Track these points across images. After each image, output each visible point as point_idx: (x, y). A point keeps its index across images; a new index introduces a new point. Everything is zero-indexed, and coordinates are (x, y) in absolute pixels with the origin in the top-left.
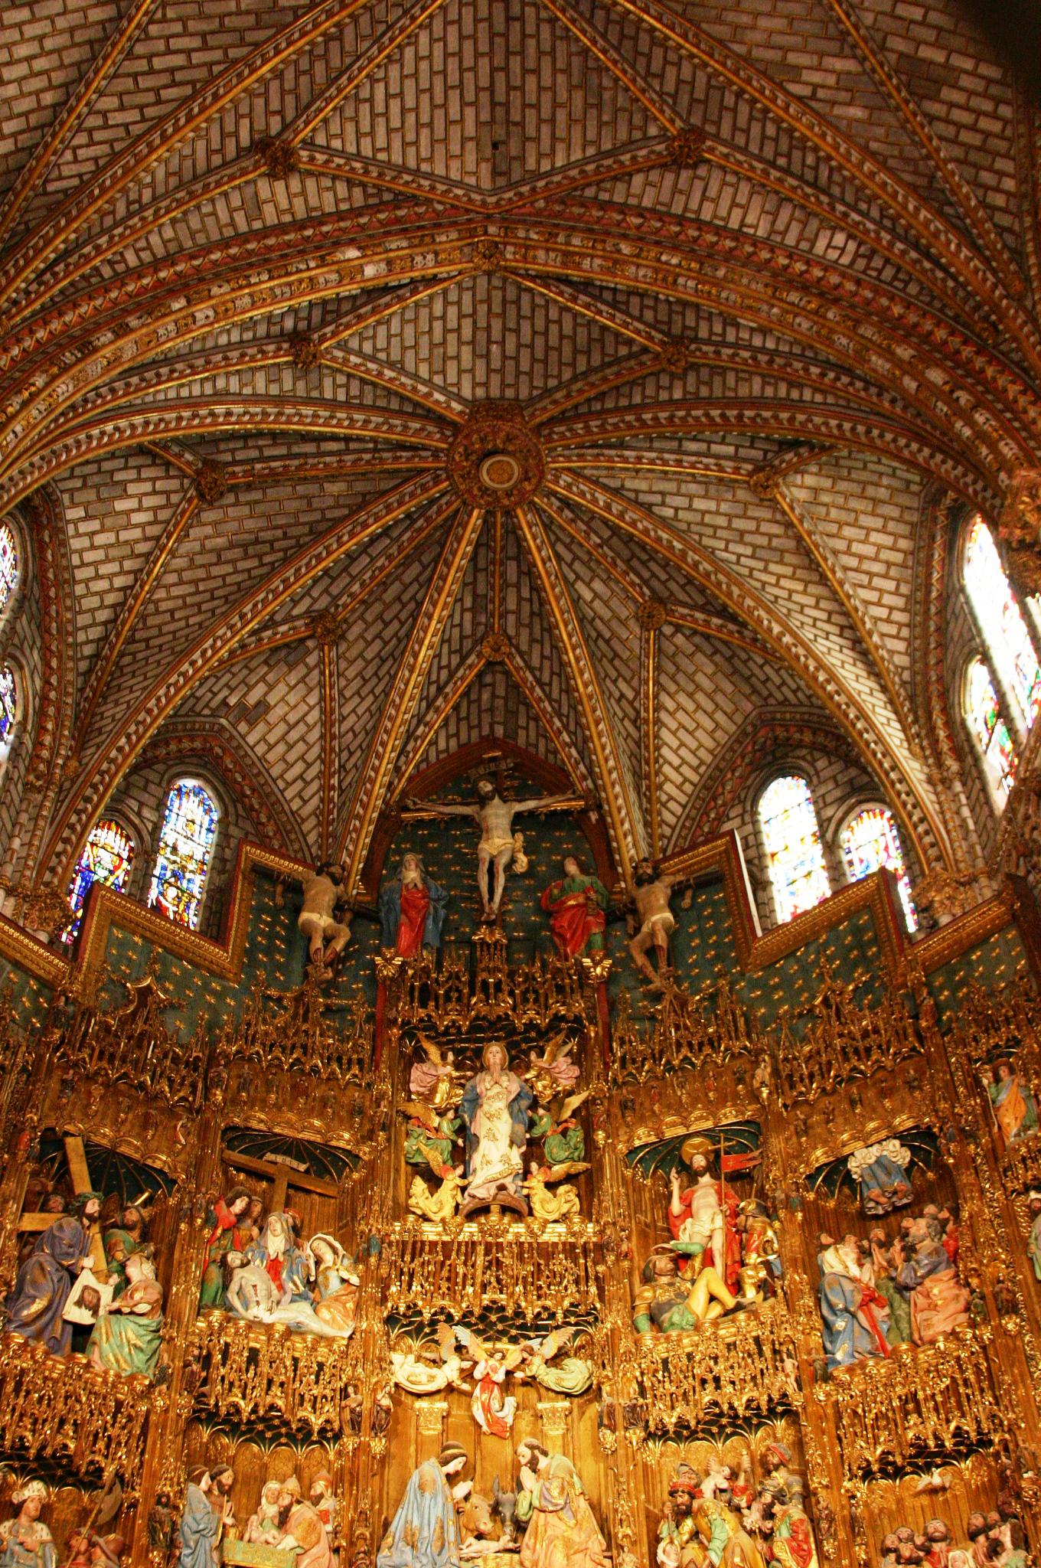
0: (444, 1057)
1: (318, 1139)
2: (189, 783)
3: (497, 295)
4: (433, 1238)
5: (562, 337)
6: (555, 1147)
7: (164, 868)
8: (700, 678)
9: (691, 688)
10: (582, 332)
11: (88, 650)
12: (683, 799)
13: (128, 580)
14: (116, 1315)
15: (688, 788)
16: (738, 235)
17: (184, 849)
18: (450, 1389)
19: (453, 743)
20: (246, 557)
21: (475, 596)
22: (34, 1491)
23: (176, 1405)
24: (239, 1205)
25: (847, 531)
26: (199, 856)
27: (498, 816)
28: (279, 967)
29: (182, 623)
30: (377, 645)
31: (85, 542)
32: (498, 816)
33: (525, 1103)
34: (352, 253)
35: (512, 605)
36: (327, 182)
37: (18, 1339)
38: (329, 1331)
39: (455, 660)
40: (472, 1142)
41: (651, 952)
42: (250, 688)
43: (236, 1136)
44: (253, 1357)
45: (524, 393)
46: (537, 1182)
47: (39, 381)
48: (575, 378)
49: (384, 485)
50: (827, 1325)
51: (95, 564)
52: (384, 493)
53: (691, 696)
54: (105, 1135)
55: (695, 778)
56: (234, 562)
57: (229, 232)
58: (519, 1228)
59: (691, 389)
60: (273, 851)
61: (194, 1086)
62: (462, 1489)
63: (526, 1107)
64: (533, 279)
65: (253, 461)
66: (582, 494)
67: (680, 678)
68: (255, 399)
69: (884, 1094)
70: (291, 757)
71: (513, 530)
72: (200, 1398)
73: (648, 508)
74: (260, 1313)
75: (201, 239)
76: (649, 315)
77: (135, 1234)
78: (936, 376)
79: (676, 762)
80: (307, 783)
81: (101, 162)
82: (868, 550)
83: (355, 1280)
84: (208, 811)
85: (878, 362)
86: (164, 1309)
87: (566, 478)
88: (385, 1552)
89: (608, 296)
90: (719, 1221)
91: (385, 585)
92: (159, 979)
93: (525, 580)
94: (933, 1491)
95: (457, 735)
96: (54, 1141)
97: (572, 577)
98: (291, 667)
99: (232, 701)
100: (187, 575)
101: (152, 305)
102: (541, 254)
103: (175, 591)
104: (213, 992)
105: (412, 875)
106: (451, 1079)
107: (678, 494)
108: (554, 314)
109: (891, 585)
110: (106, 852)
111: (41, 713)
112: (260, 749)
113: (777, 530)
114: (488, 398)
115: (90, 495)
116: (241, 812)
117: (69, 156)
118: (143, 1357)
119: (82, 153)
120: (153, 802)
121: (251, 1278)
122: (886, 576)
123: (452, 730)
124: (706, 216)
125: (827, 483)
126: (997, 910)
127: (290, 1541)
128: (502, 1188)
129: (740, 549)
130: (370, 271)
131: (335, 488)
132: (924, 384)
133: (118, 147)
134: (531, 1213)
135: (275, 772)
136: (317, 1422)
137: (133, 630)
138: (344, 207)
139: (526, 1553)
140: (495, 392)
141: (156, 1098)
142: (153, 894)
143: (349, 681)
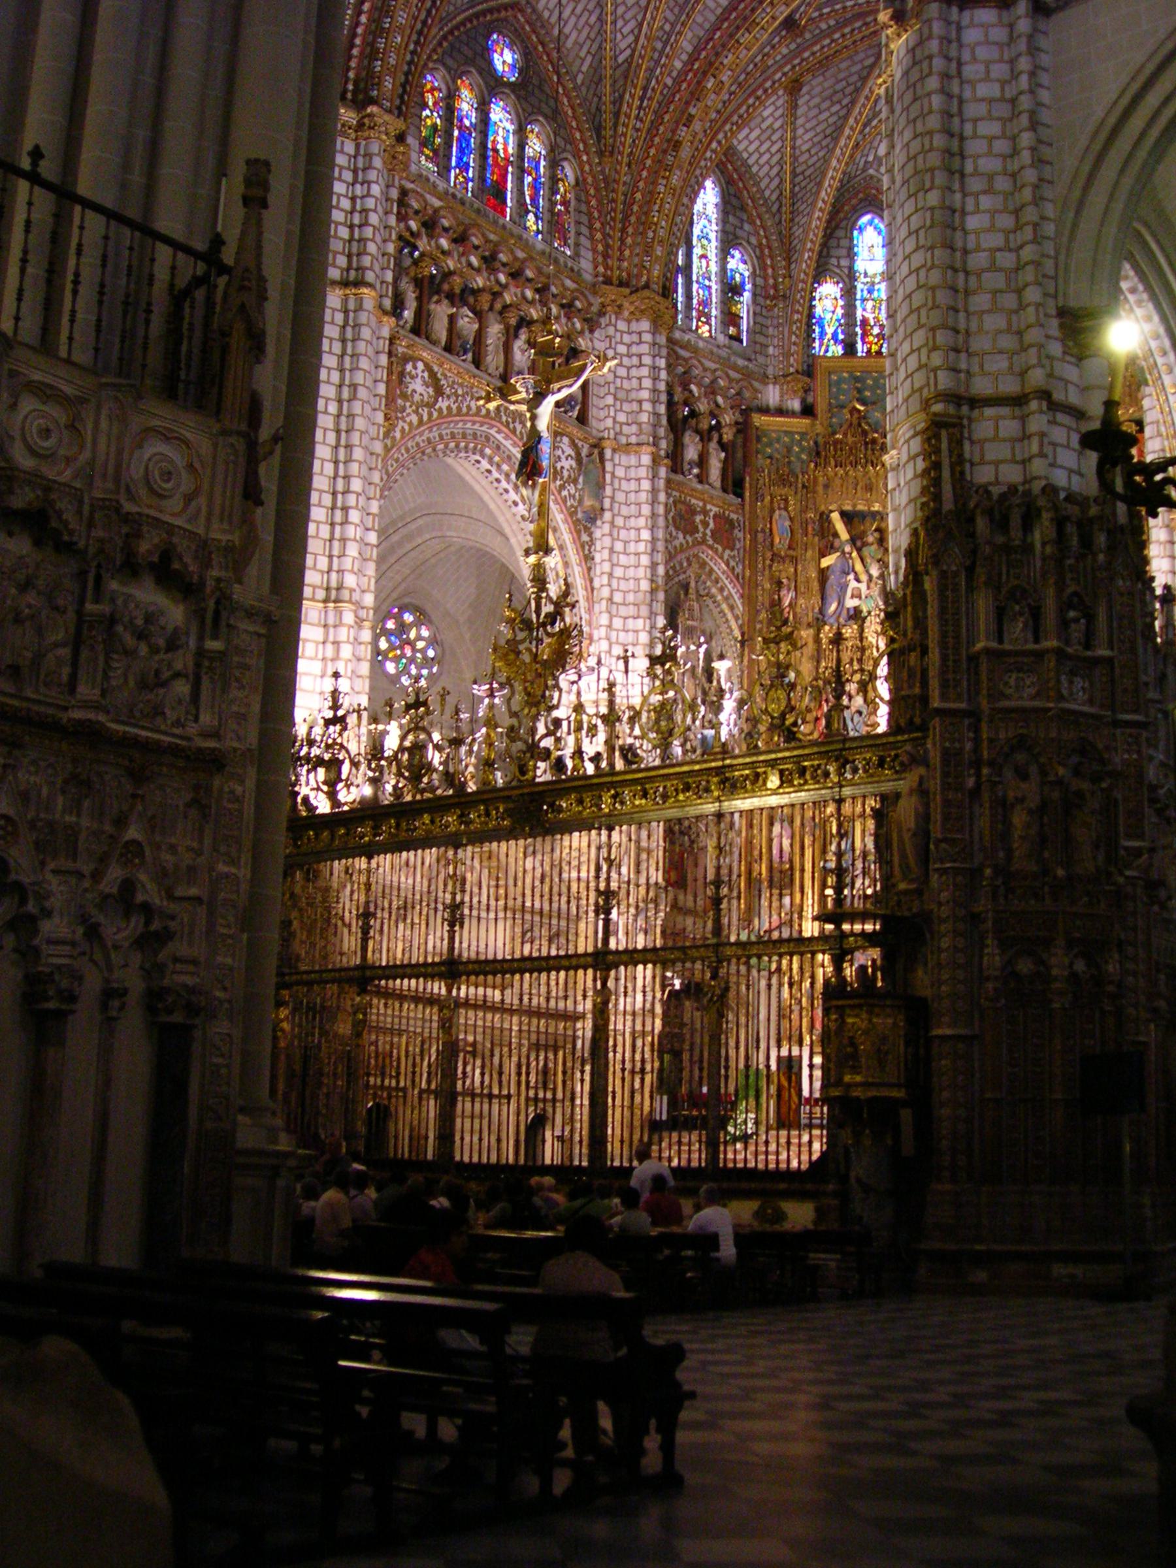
2: (865, 219)
11: (774, 197)
13: (779, 145)
20: (833, 104)
31: (746, 143)
51: (757, 149)
56: (828, 109)
68: (787, 59)
75: (707, 26)
100: (808, 126)
101: (697, 94)
103: (806, 137)
111: (761, 258)
117: (619, 36)
120: (844, 252)
133: (639, 18)
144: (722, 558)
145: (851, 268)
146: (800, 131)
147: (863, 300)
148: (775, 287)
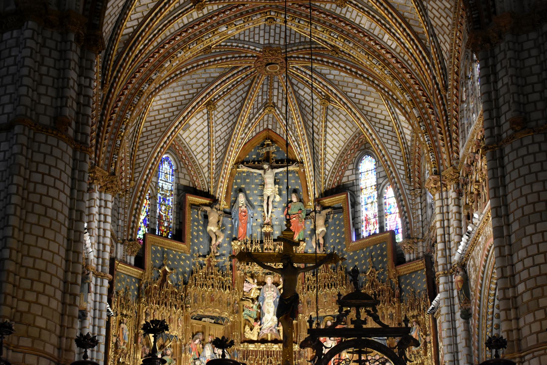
4: (252, 349)
7: (160, 198)
8: (341, 116)
9: (338, 119)
12: (333, 160)
15: (335, 156)
17: (165, 187)
20: (183, 90)
21: (263, 92)
28: (201, 243)
29: (162, 116)
32: (269, 177)
53: (337, 122)
56: (179, 92)
67: (334, 116)
70: (199, 143)
79: (331, 146)
81: (140, 20)
97: (297, 89)
103: (159, 103)
114: (269, 43)
116: (182, 166)
119: (133, 17)
133: (145, 13)
135: (193, 149)
140: (272, 41)
143: (218, 119)
145: (157, 183)
147: (160, 204)
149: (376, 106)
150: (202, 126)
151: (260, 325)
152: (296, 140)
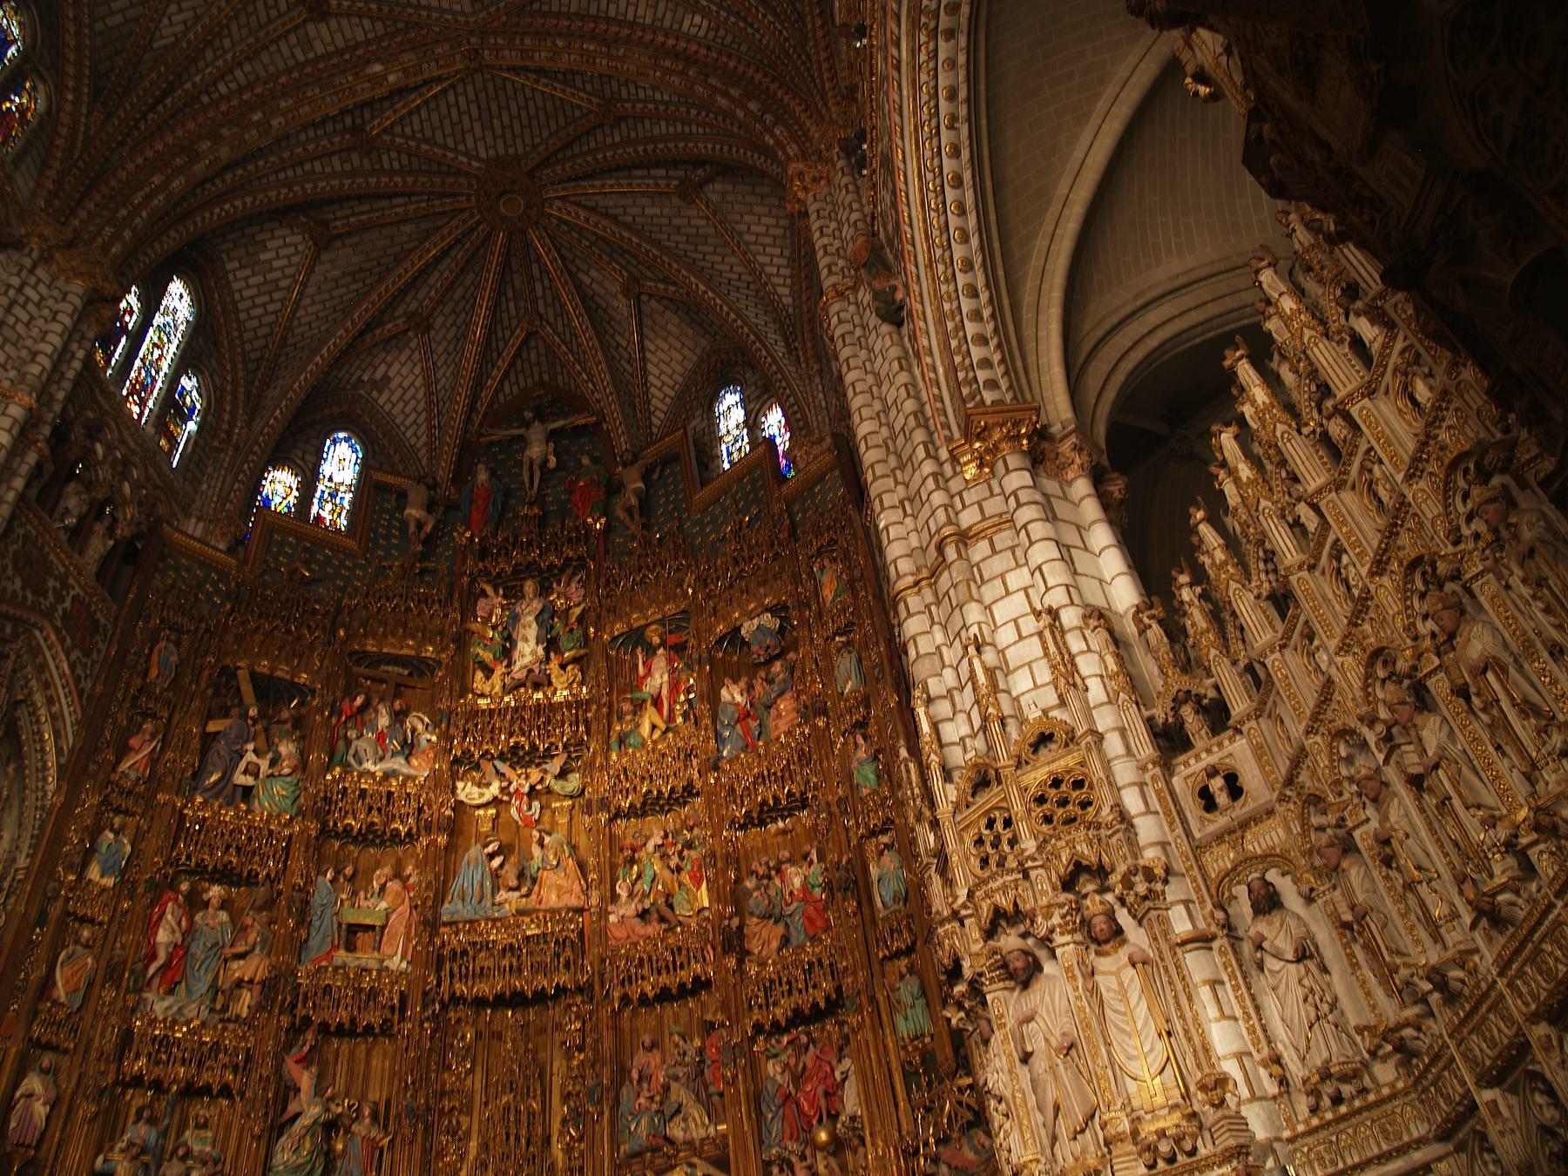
0: (496, 592)
1: (413, 653)
2: (341, 435)
3: (490, 85)
5: (537, 109)
6: (564, 642)
8: (670, 327)
10: (549, 104)
12: (665, 408)
13: (278, 306)
14: (269, 778)
15: (668, 400)
16: (633, 25)
18: (495, 801)
19: (515, 389)
20: (355, 281)
22: (215, 891)
23: (308, 828)
24: (359, 701)
25: (747, 218)
26: (348, 482)
27: (536, 433)
30: (454, 329)
32: (536, 433)
33: (546, 616)
34: (378, 68)
35: (539, 293)
36: (355, 20)
37: (199, 799)
38: (413, 772)
39: (508, 333)
40: (514, 644)
41: (629, 511)
42: (376, 368)
43: (362, 657)
44: (363, 793)
45: (520, 150)
46: (554, 666)
47: (157, 180)
48: (551, 135)
49: (440, 223)
50: (718, 737)
51: (252, 298)
52: (439, 228)
53: (665, 340)
54: (264, 666)
55: (672, 394)
57: (292, 63)
58: (540, 695)
59: (625, 134)
60: (396, 473)
61: (324, 627)
62: (496, 862)
63: (546, 618)
64: (508, 70)
65: (347, 217)
66: (569, 213)
69: (764, 583)
70: (407, 410)
71: (528, 244)
72: (325, 823)
73: (614, 219)
74: (369, 766)
75: (272, 69)
76: (589, 87)
77: (289, 726)
78: (753, 106)
79: (659, 384)
80: (419, 426)
82: (761, 229)
83: (434, 738)
84: (355, 451)
85: (722, 102)
86: (304, 770)
87: (558, 203)
88: (446, 905)
89: (560, 77)
90: (666, 677)
91: (451, 287)
92: (307, 564)
93: (545, 276)
94: (784, 832)
95: (517, 382)
96: (229, 674)
98: (401, 351)
99: (366, 378)
100: (317, 298)
102: (507, 53)
103: (310, 310)
104: (348, 568)
105: (483, 476)
106: (502, 607)
107: (634, 205)
108: (528, 93)
109: (777, 251)
110: (280, 486)
111: (220, 401)
112: (388, 407)
113: (702, 222)
115: (242, 252)
117: (166, 21)
118: (289, 802)
121: (365, 743)
122: (774, 245)
123: (513, 379)
124: (612, 13)
125: (729, 187)
126: (828, 458)
127: (383, 905)
128: (530, 671)
129: (678, 238)
130: (392, 78)
131: (407, 229)
132: (748, 112)
133: (199, 11)
134: (550, 683)
135: (398, 421)
136: (403, 830)
137: (284, 338)
138: (371, 36)
139: (534, 896)
140: (501, 151)
141: (299, 638)
142: (315, 509)
144: (68, 655)
146: (307, 301)
148: (229, 433)
149: (719, 259)
150: (412, 377)
151: (509, 665)
152: (584, 370)
